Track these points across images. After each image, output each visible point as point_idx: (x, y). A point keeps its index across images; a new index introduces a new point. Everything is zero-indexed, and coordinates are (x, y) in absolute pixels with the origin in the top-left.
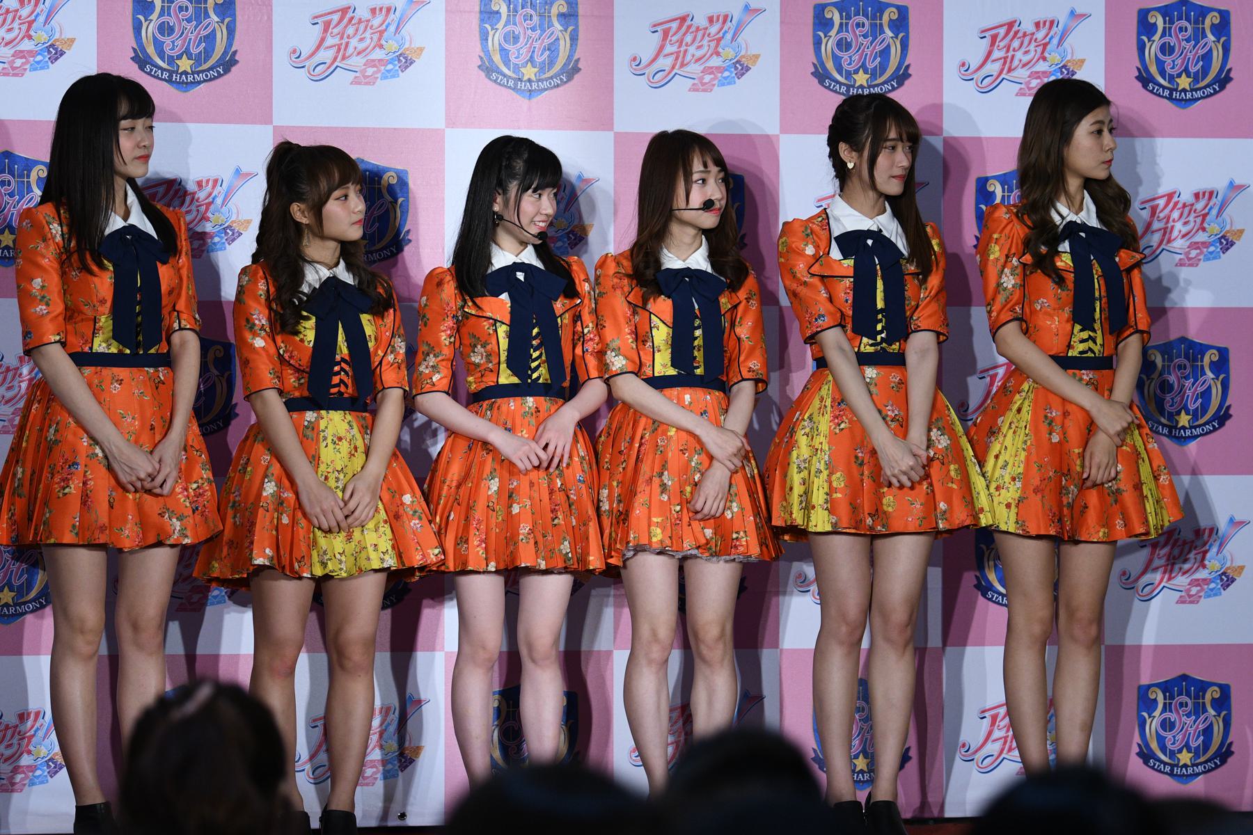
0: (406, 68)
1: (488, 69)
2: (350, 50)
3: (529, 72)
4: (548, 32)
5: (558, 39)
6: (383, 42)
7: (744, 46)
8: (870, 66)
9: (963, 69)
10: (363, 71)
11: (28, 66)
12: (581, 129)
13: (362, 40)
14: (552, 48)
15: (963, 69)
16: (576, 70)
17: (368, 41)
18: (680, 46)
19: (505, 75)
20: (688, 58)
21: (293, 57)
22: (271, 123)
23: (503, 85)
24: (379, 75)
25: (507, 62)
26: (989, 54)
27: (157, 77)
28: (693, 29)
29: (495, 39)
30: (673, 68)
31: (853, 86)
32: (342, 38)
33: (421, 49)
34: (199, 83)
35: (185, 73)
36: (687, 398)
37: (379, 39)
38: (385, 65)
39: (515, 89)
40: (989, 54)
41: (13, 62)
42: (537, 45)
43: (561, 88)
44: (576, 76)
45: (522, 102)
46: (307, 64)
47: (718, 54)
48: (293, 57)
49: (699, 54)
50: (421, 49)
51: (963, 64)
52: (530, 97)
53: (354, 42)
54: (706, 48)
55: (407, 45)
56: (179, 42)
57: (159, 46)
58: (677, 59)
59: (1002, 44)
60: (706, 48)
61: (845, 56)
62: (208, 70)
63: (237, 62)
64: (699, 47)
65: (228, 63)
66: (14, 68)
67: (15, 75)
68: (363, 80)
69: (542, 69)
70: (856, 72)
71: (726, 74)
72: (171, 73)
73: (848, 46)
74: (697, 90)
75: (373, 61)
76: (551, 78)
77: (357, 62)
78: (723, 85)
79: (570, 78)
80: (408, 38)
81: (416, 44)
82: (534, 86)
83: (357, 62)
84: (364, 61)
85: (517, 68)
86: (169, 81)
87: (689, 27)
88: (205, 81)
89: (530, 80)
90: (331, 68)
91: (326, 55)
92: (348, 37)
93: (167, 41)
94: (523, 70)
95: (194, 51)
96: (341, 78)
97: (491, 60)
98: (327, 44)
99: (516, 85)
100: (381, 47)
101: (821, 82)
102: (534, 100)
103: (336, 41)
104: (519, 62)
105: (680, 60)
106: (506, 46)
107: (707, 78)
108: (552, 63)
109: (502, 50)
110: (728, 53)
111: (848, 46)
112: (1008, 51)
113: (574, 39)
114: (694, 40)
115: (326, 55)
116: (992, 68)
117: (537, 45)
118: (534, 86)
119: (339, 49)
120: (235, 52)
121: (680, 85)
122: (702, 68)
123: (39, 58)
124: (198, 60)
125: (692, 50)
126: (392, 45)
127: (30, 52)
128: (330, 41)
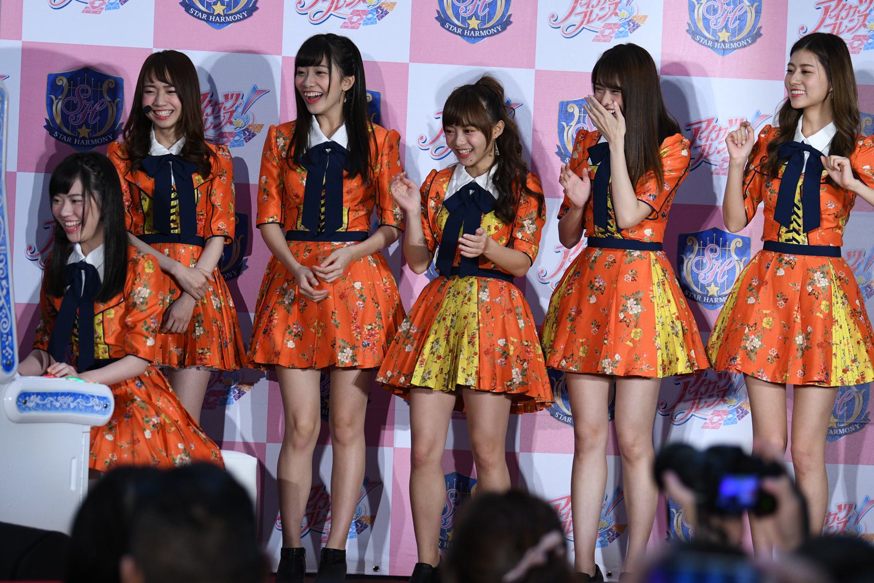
0: (634, 30)
1: (694, 33)
2: (594, 16)
3: (724, 36)
4: (739, 7)
5: (746, 12)
6: (618, 11)
11: (361, 22)
12: (760, 78)
13: (602, 9)
14: (742, 19)
16: (759, 35)
17: (607, 10)
18: (837, 20)
19: (705, 38)
21: (552, 20)
22: (534, 67)
23: (704, 45)
24: (613, 35)
25: (707, 28)
27: (454, 32)
28: (847, 7)
29: (700, 11)
32: (588, 7)
33: (645, 17)
34: (483, 37)
35: (474, 29)
36: (167, 251)
37: (615, 9)
39: (712, 48)
41: (351, 18)
42: (730, 16)
43: (747, 48)
44: (758, 40)
45: (718, 57)
46: (562, 25)
47: (865, 26)
48: (552, 20)
50: (645, 17)
52: (724, 54)
53: (596, 10)
54: (856, 22)
55: (635, 14)
56: (470, 7)
57: (455, 9)
60: (856, 22)
62: (490, 28)
63: (511, 23)
64: (851, 21)
65: (505, 23)
66: (352, 23)
67: (352, 28)
69: (733, 34)
72: (463, 29)
75: (610, 24)
76: (740, 40)
77: (598, 25)
80: (636, 9)
81: (642, 14)
82: (727, 46)
83: (598, 25)
85: (715, 33)
86: (462, 35)
87: (844, 5)
88: (488, 36)
89: (724, 42)
90: (579, 29)
91: (576, 19)
92: (593, 7)
93: (462, 6)
95: (481, 14)
97: (696, 26)
98: (577, 11)
99: (713, 45)
100: (616, 14)
102: (727, 56)
103: (584, 9)
104: (717, 28)
106: (708, 16)
108: (741, 29)
109: (704, 18)
113: (758, 12)
114: (847, 16)
115: (576, 19)
117: (730, 16)
118: (727, 46)
119: (585, 16)
120: (510, 15)
123: (370, 16)
124: (484, 20)
126: (624, 13)
127: (363, 11)
128: (579, 9)
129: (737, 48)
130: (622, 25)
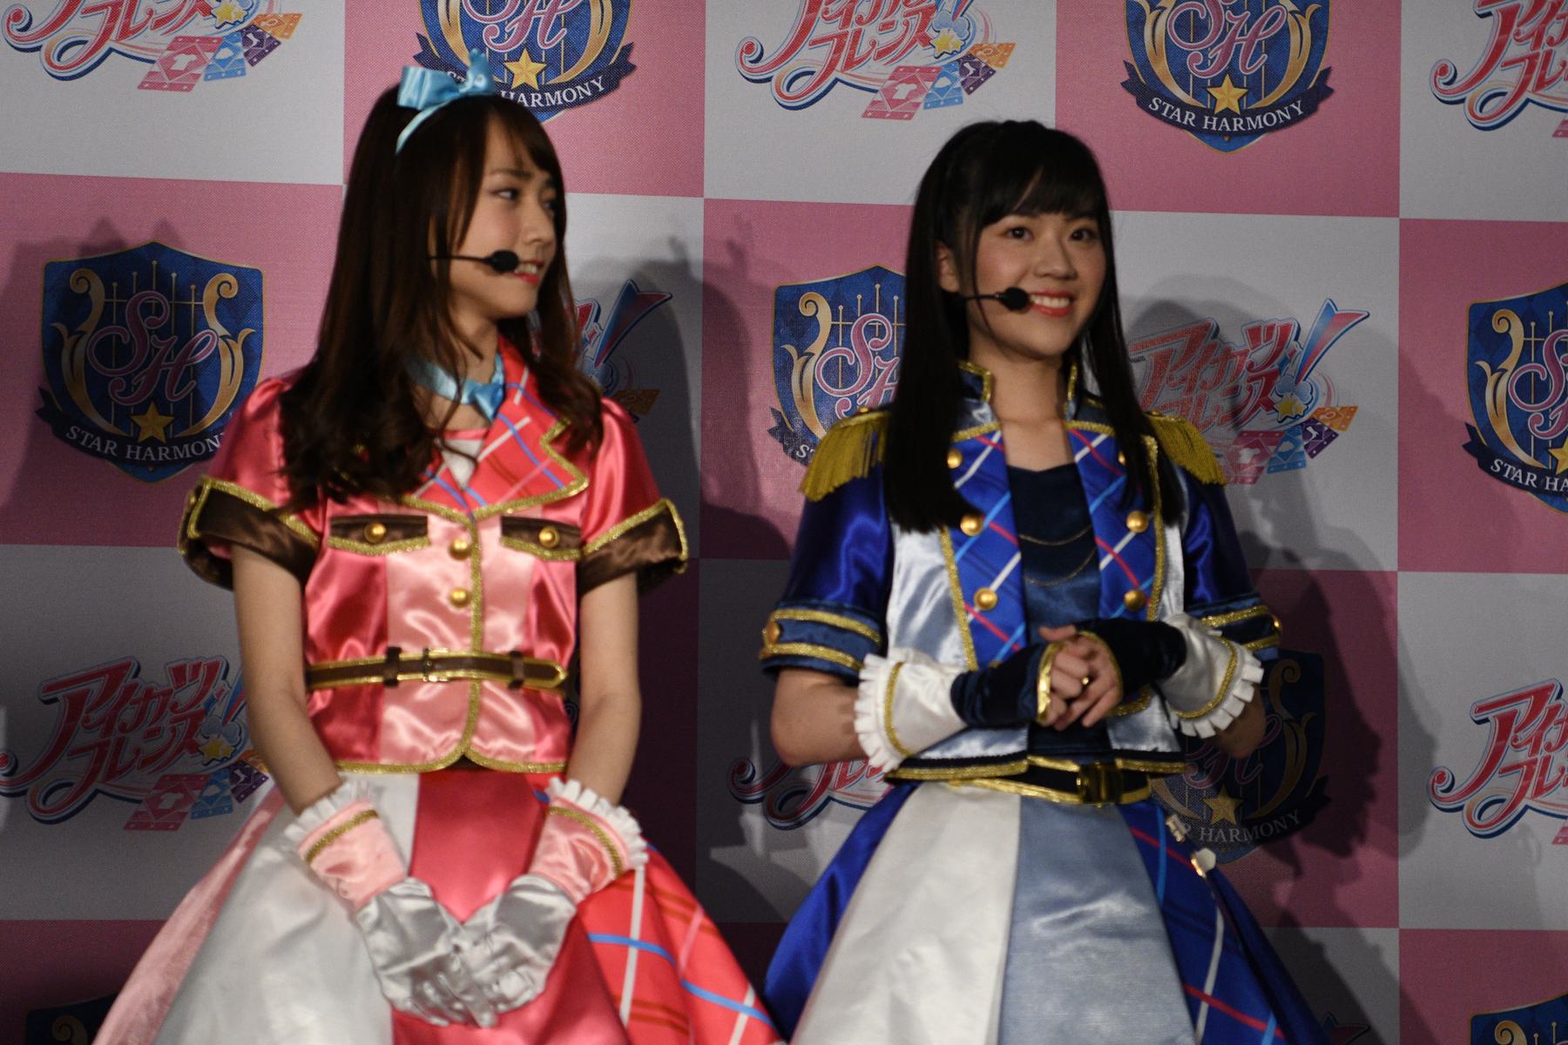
0: (262, 55)
7: (980, 25)
8: (1247, 70)
9: (1441, 80)
10: (170, 61)
15: (1441, 80)
20: (864, 47)
21: (15, 27)
24: (201, 70)
26: (1499, 48)
30: (831, 67)
31: (1211, 113)
33: (295, 18)
38: (215, 50)
40: (1499, 48)
44: (624, 82)
47: (926, 41)
49: (886, 39)
50: (295, 18)
51: (1443, 70)
58: (838, 50)
59: (1525, 29)
60: (900, 29)
61: (1193, 49)
64: (886, 27)
68: (167, 79)
70: (1217, 83)
71: (943, 82)
73: (1201, 29)
74: (881, 115)
75: (192, 39)
76: (572, 83)
78: (936, 105)
79: (611, 85)
83: (154, 41)
84: (169, 39)
90: (97, 55)
94: (511, 66)
96: (119, 74)
101: (1143, 103)
105: (845, 51)
107: (903, 91)
108: (573, 51)
109: (465, 20)
110: (947, 39)
111: (1201, 29)
112: (1537, 44)
116: (1505, 78)
117: (541, 14)
121: (844, 103)
122: (891, 69)
125: (870, 31)
129: (565, 106)
130: (222, 43)
